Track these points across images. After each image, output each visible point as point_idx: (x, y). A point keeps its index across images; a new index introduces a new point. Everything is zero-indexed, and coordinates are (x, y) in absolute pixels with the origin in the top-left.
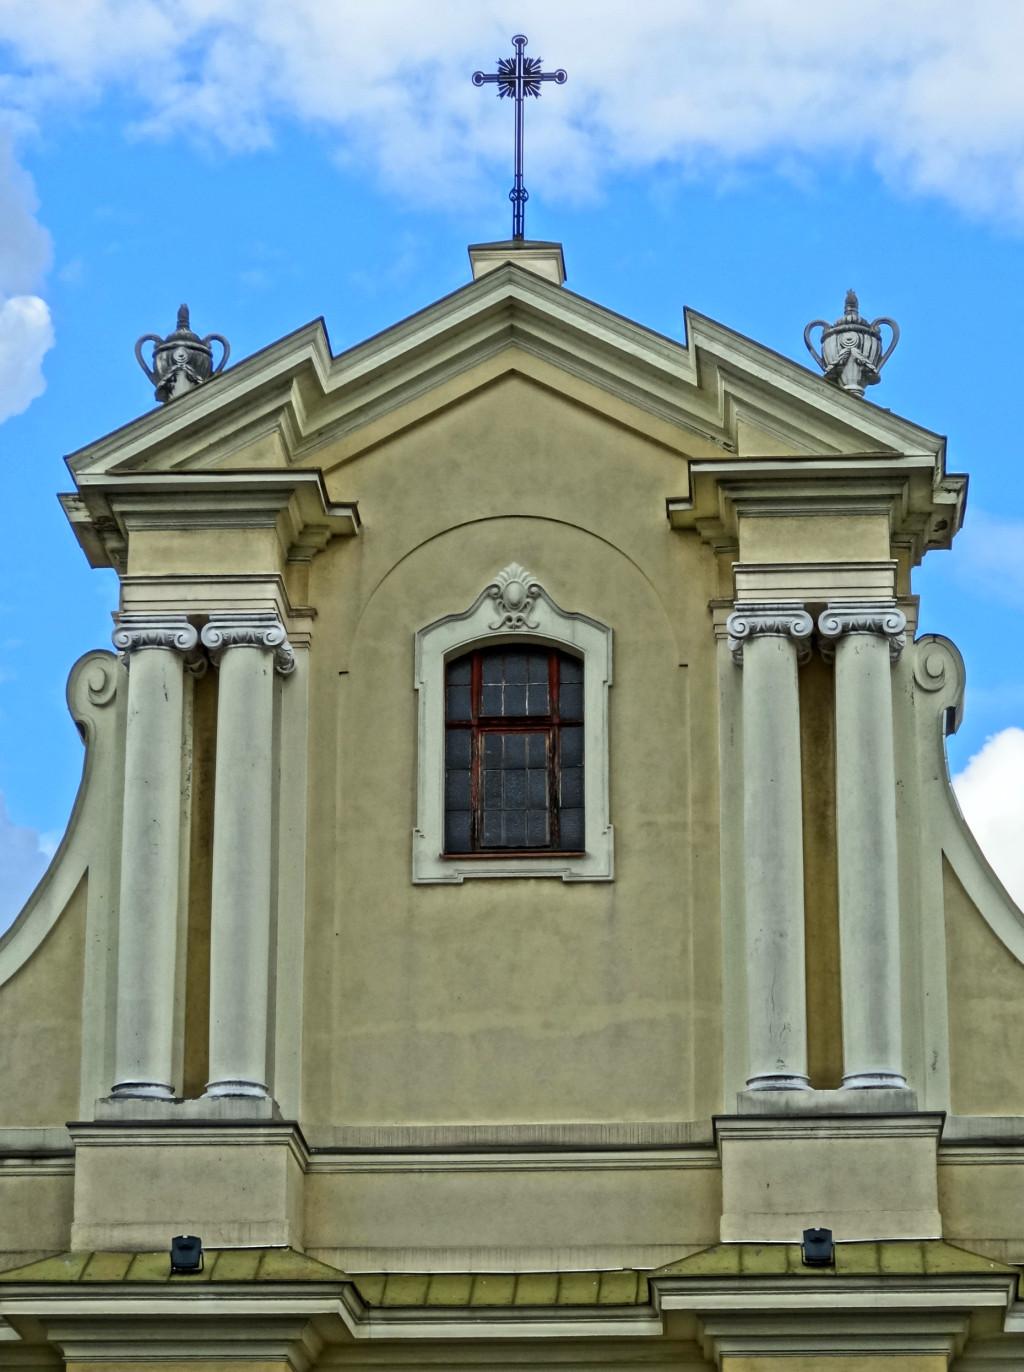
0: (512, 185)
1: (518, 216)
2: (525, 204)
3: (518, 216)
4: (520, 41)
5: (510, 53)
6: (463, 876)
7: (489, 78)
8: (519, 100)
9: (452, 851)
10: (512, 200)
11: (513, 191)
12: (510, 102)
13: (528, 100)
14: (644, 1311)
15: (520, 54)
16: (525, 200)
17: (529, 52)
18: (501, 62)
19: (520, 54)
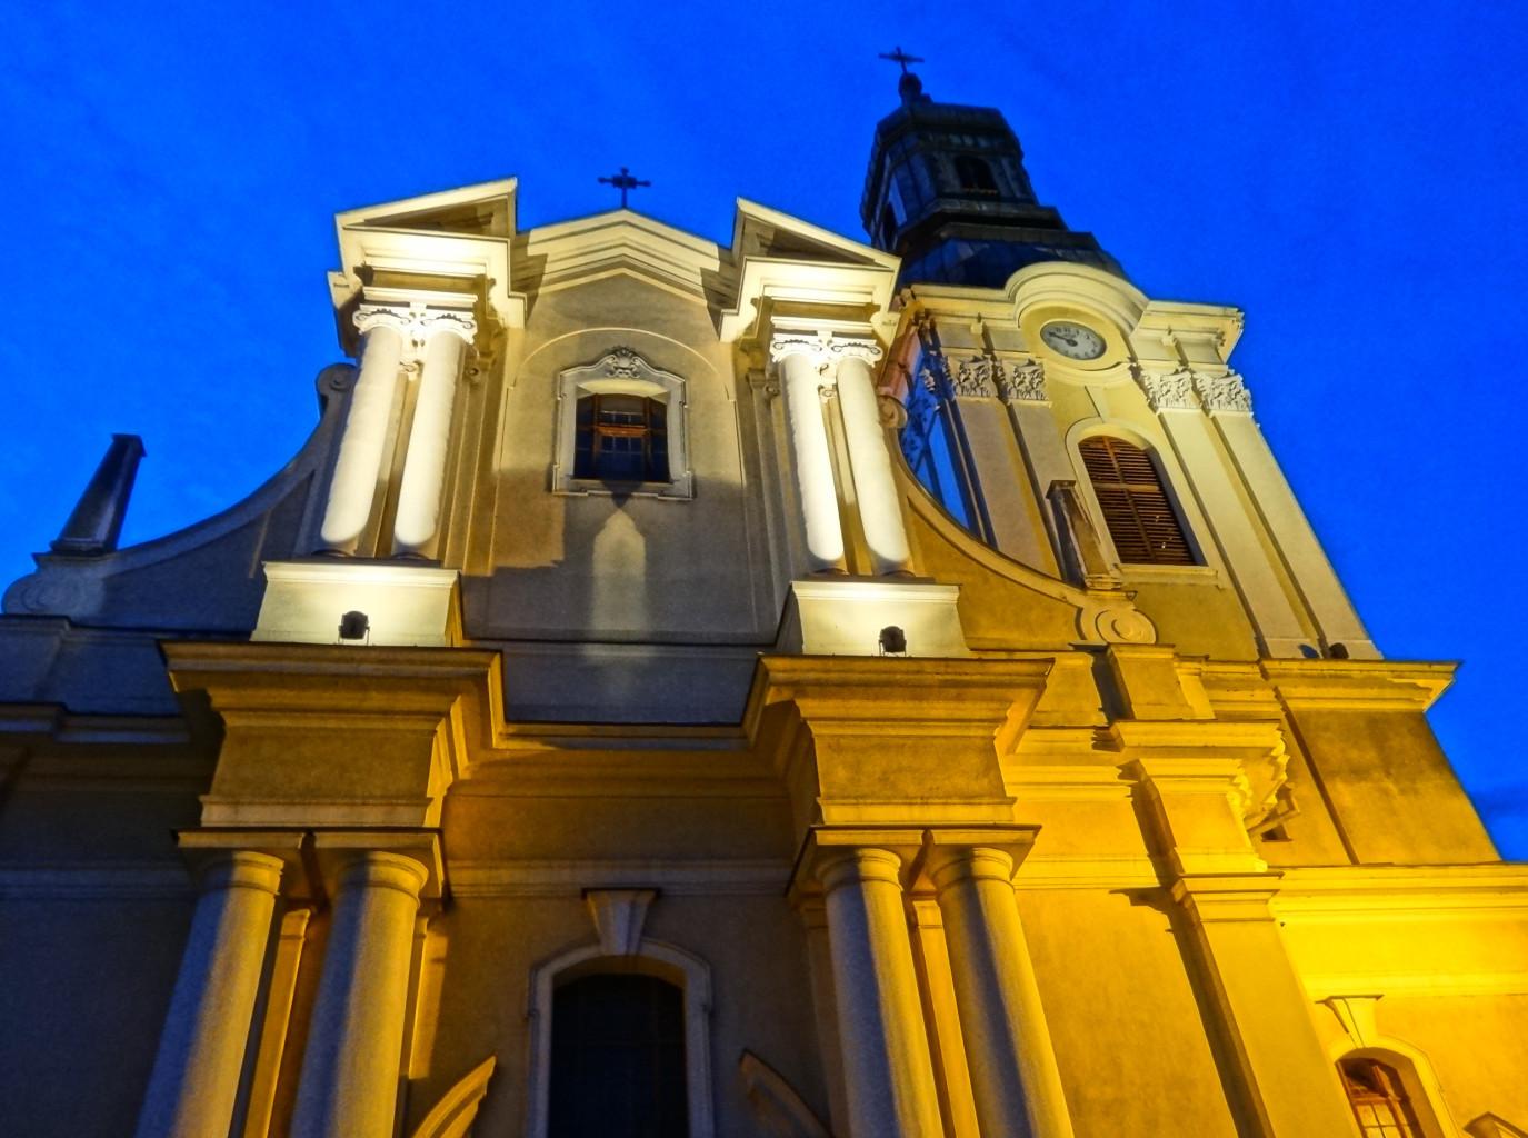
14: (735, 732)
17: (629, 175)
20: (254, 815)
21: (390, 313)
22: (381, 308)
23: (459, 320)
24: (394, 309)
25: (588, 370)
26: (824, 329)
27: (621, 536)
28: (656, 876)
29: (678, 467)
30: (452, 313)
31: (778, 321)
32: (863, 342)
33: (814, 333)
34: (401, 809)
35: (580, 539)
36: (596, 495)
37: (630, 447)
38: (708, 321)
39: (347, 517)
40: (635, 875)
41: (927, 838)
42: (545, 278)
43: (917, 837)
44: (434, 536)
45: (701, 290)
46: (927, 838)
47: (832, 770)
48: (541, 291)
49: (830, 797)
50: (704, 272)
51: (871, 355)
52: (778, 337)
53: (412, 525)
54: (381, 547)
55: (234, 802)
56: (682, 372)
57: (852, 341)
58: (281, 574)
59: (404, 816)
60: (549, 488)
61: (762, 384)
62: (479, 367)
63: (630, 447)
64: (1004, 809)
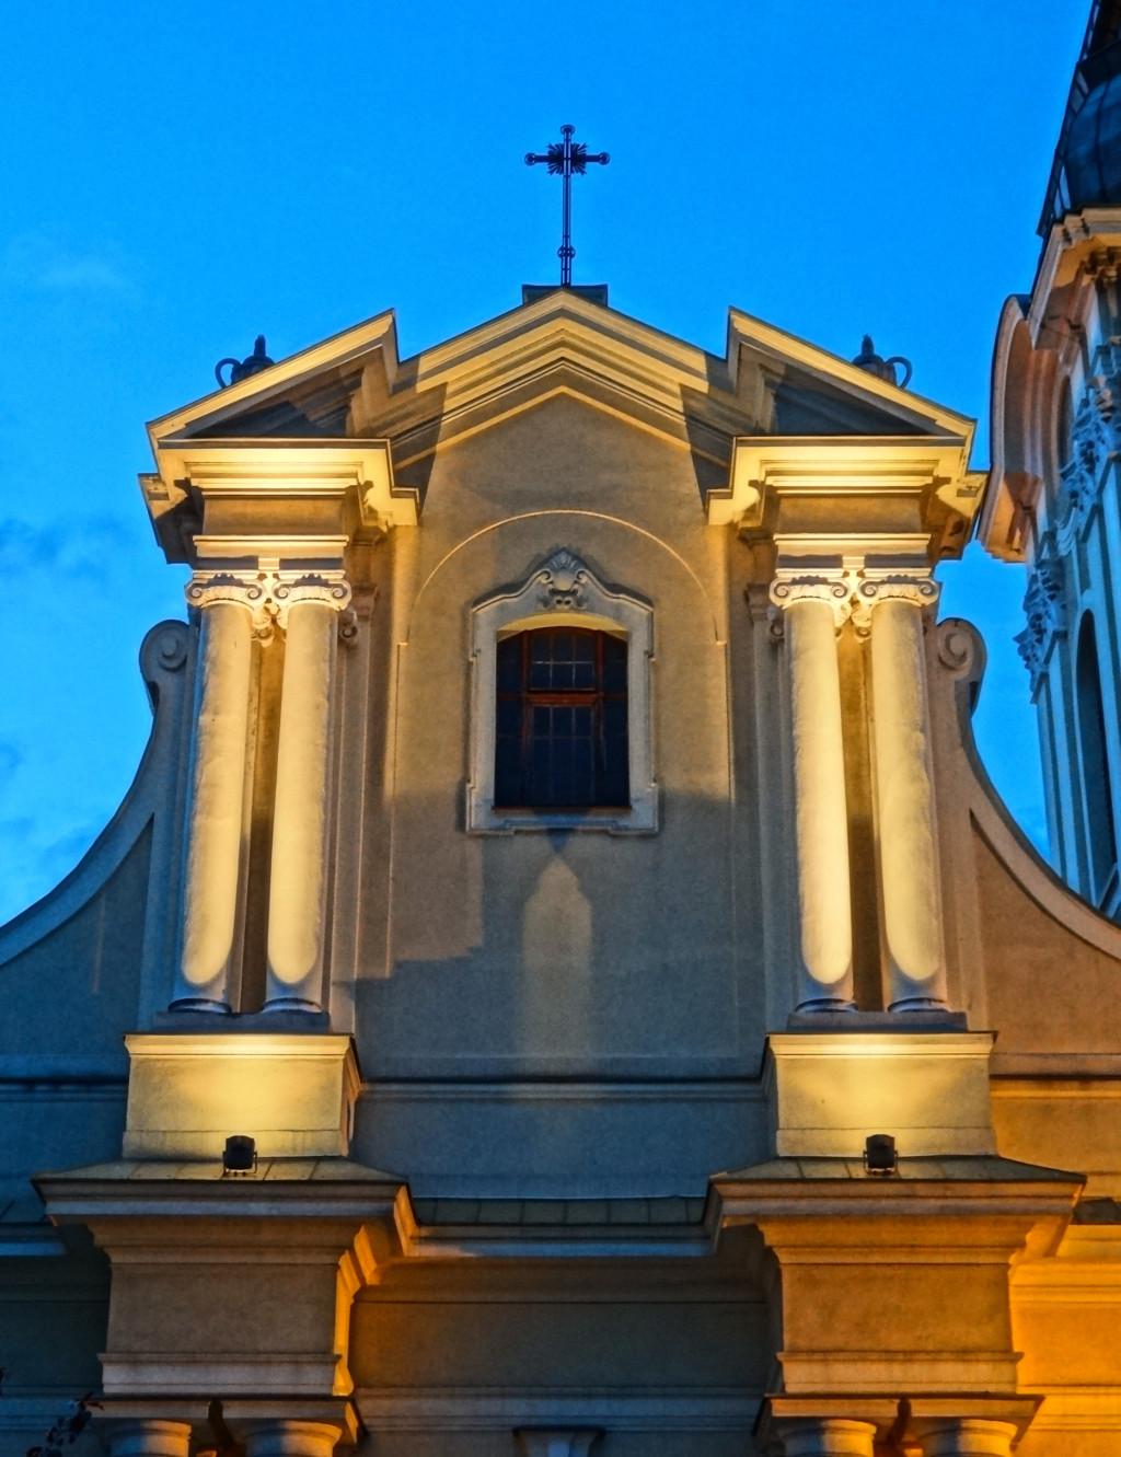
0: (560, 243)
1: (566, 269)
2: (573, 260)
3: (566, 269)
4: (568, 130)
5: (559, 139)
6: (514, 828)
7: (540, 159)
8: (567, 177)
9: (506, 797)
10: (561, 256)
11: (562, 249)
12: (558, 178)
13: (575, 177)
14: (696, 1231)
15: (567, 140)
16: (572, 256)
17: (576, 139)
18: (550, 147)
19: (567, 140)
20: (158, 1379)
21: (240, 584)
22: (219, 573)
23: (325, 584)
24: (239, 574)
25: (511, 600)
26: (854, 551)
27: (564, 890)
28: (599, 1410)
29: (640, 783)
30: (316, 573)
31: (788, 543)
32: (910, 572)
33: (834, 561)
34: (308, 1368)
35: (506, 908)
36: (526, 838)
37: (574, 729)
38: (690, 486)
39: (209, 955)
40: (574, 1410)
41: (904, 1410)
42: (446, 421)
43: (890, 1410)
44: (314, 968)
45: (681, 420)
46: (904, 1410)
47: (799, 1314)
48: (439, 447)
49: (795, 1351)
50: (687, 392)
51: (920, 596)
52: (785, 574)
53: (290, 954)
54: (253, 1003)
55: (133, 1360)
56: (650, 592)
57: (894, 572)
58: (142, 1048)
59: (310, 1380)
60: (461, 823)
61: (763, 641)
62: (357, 640)
63: (574, 729)
64: (1005, 1368)
